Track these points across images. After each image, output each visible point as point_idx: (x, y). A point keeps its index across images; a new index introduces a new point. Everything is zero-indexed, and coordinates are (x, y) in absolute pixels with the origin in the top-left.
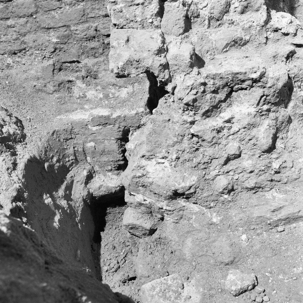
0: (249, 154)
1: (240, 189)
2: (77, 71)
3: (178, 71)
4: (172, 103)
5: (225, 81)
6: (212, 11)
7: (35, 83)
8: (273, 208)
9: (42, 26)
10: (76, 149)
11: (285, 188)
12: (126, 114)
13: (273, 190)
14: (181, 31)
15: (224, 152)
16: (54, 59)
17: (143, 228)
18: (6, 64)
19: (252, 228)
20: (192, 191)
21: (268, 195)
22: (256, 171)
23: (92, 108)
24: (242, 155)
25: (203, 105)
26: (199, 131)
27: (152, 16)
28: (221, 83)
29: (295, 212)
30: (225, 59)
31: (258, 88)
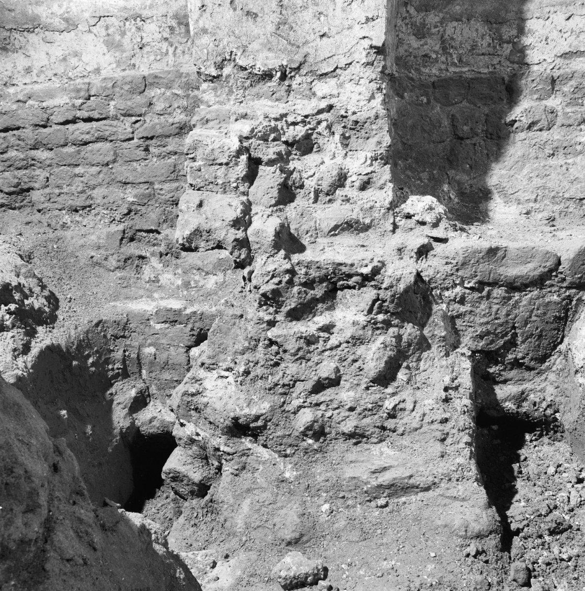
0: (351, 383)
1: (333, 435)
2: (154, 245)
3: (260, 251)
4: (248, 293)
5: (324, 272)
6: (320, 182)
7: (93, 254)
8: (373, 468)
9: (118, 180)
10: (127, 353)
11: (401, 442)
12: (204, 310)
13: (384, 443)
14: (273, 202)
15: (314, 373)
16: (126, 224)
17: (189, 480)
18: (61, 223)
19: (341, 496)
20: (260, 423)
21: (376, 449)
22: (359, 410)
23: (162, 298)
24: (342, 382)
25: (288, 301)
26: (279, 336)
27: (238, 179)
28: (317, 274)
29: (403, 476)
30: (330, 244)
31: (371, 288)
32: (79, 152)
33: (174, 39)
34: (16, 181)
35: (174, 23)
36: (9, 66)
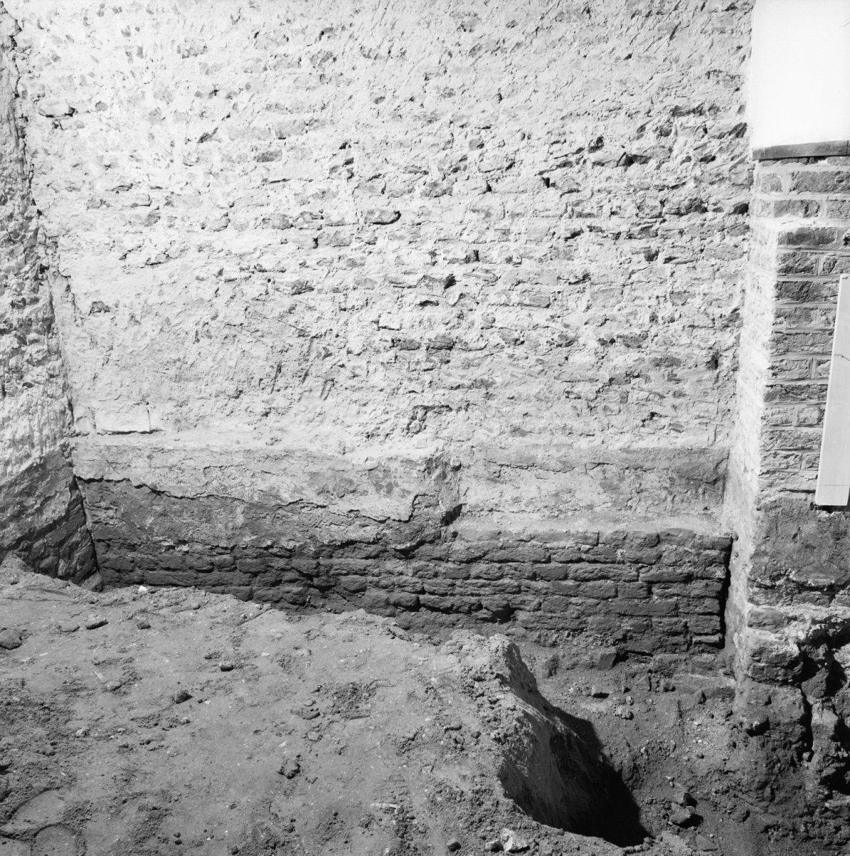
32: (579, 586)
33: (676, 489)
34: (505, 602)
35: (675, 476)
36: (497, 495)
